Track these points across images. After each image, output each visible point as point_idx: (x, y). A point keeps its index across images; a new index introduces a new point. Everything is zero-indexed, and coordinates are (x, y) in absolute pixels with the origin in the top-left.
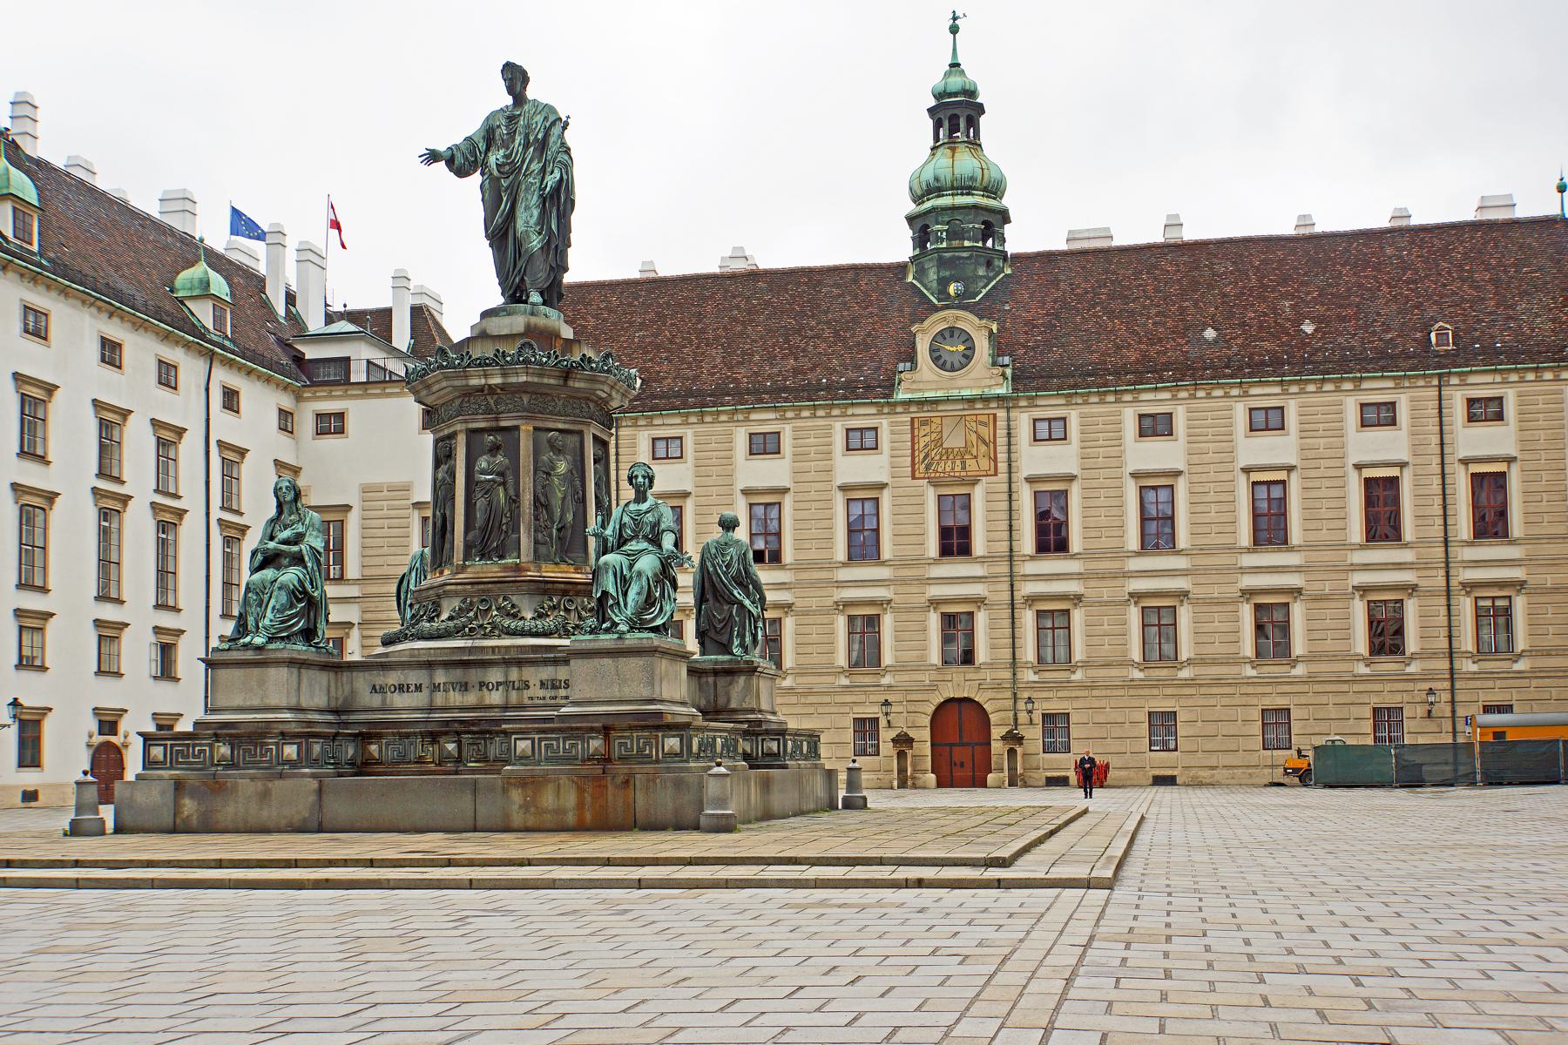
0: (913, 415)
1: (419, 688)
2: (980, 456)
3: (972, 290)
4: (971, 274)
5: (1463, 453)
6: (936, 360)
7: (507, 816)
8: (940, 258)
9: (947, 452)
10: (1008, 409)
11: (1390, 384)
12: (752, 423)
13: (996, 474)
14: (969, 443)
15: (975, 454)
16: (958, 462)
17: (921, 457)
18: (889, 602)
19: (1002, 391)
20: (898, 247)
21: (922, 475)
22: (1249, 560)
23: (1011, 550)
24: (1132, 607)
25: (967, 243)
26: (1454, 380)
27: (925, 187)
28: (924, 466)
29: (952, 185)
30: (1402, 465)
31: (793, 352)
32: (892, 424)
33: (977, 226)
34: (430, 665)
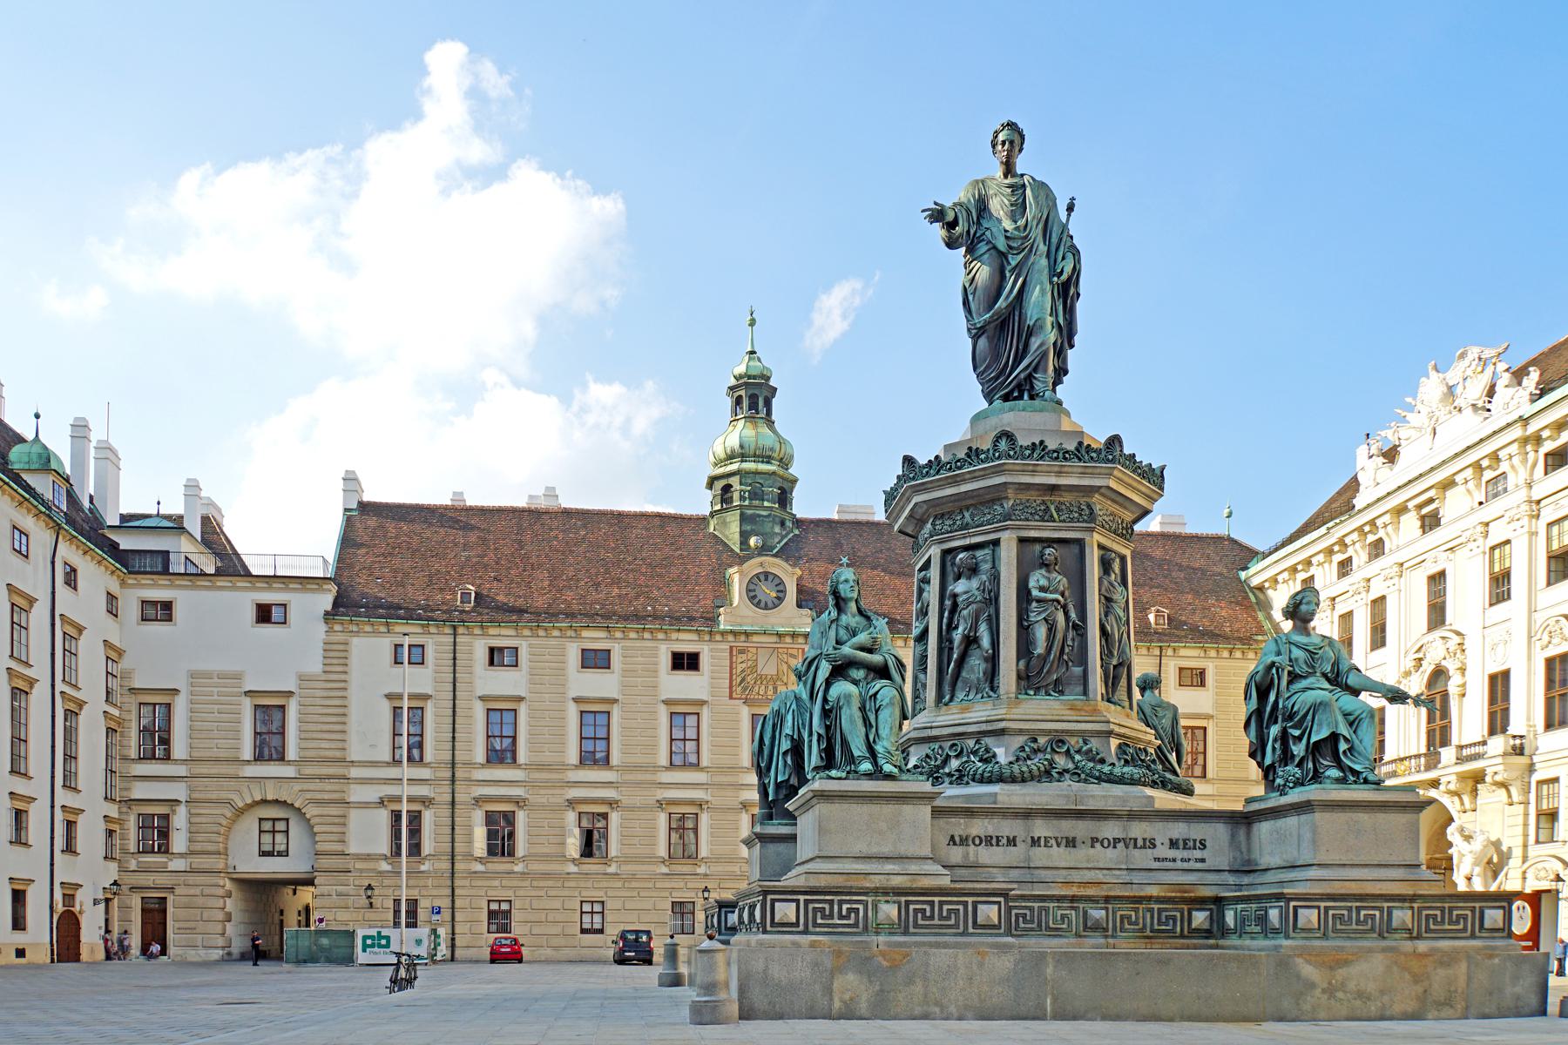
1: (1012, 842)
3: (769, 544)
4: (768, 530)
6: (752, 598)
8: (742, 515)
9: (761, 678)
12: (583, 640)
14: (780, 672)
15: (785, 681)
16: (771, 687)
17: (739, 679)
20: (700, 503)
21: (739, 696)
25: (766, 504)
27: (729, 451)
28: (740, 688)
29: (755, 454)
31: (616, 582)
32: (711, 650)
33: (775, 490)
34: (1027, 814)
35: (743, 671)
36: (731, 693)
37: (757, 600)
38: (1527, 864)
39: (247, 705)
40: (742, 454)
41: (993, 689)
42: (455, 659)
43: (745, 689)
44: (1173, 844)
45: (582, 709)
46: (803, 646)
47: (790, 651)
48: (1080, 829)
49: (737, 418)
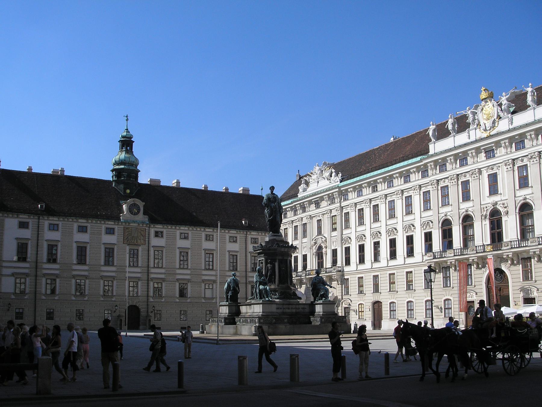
0: (124, 226)
1: (281, 309)
2: (141, 239)
6: (130, 211)
10: (149, 227)
11: (235, 232)
13: (145, 245)
15: (140, 238)
16: (135, 240)
17: (126, 238)
18: (116, 277)
20: (108, 176)
21: (126, 243)
23: (148, 265)
24: (177, 283)
26: (249, 233)
27: (120, 162)
34: (283, 304)
35: (127, 235)
36: (124, 242)
37: (132, 212)
38: (343, 300)
40: (125, 163)
41: (275, 283)
43: (128, 241)
44: (302, 308)
45: (78, 245)
46: (146, 228)
48: (290, 306)
49: (123, 150)
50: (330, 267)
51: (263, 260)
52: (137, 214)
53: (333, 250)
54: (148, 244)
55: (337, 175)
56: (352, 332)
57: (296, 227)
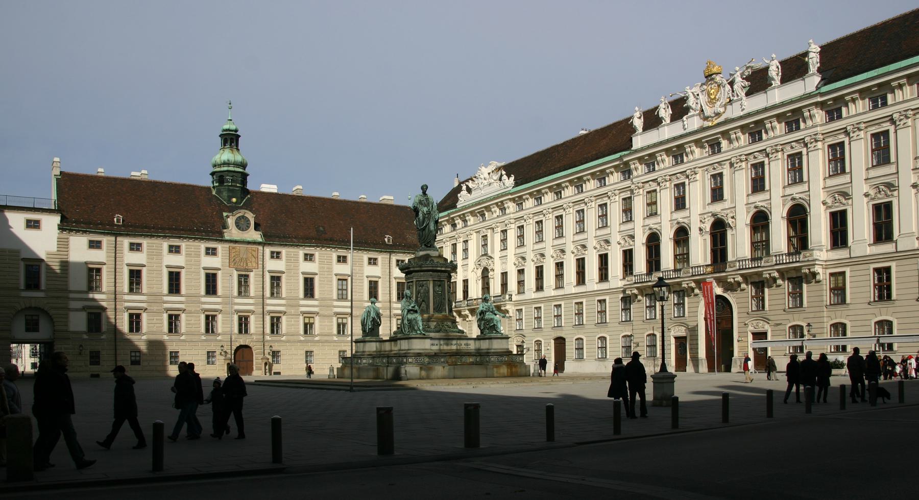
1: (437, 345)
2: (253, 261)
5: (395, 275)
7: (493, 374)
8: (228, 189)
16: (245, 263)
17: (233, 259)
19: (260, 240)
20: (207, 181)
22: (336, 303)
25: (238, 185)
27: (223, 162)
30: (380, 278)
32: (223, 247)
35: (234, 256)
36: (229, 265)
39: (22, 265)
42: (116, 247)
43: (235, 263)
47: (253, 249)
50: (500, 294)
51: (412, 282)
52: (246, 230)
53: (502, 274)
54: (262, 267)
55: (509, 176)
56: (531, 375)
57: (454, 245)
